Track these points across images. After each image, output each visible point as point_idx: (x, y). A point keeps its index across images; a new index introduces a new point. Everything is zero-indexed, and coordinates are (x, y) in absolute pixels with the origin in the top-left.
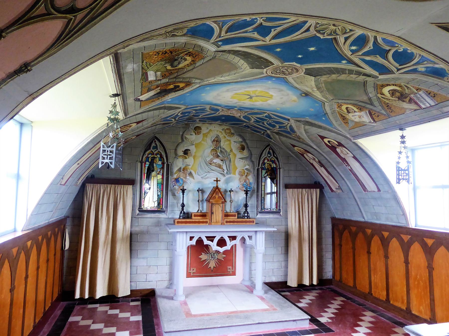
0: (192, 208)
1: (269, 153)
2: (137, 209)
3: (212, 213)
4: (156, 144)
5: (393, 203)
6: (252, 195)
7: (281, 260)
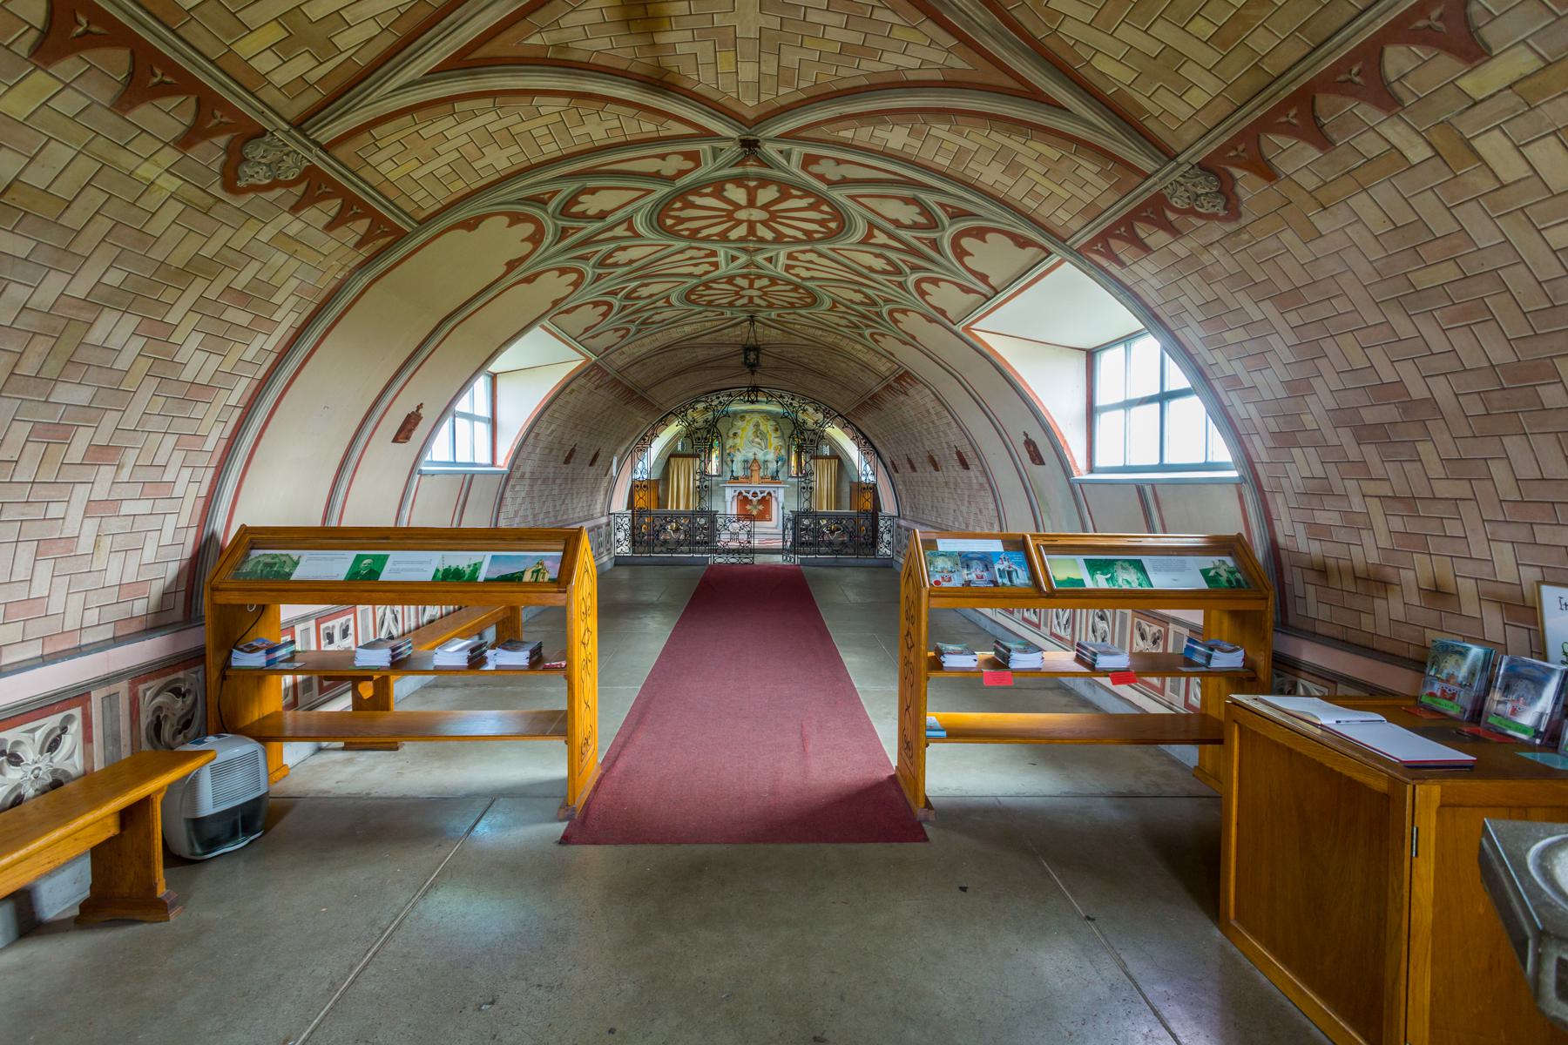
0: (739, 472)
6: (783, 465)
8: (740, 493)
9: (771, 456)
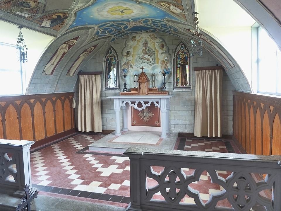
1: (182, 47)
2: (104, 87)
3: (140, 88)
4: (111, 50)
5: (241, 74)
6: (169, 77)
7: (191, 119)
8: (127, 103)
9: (158, 71)
